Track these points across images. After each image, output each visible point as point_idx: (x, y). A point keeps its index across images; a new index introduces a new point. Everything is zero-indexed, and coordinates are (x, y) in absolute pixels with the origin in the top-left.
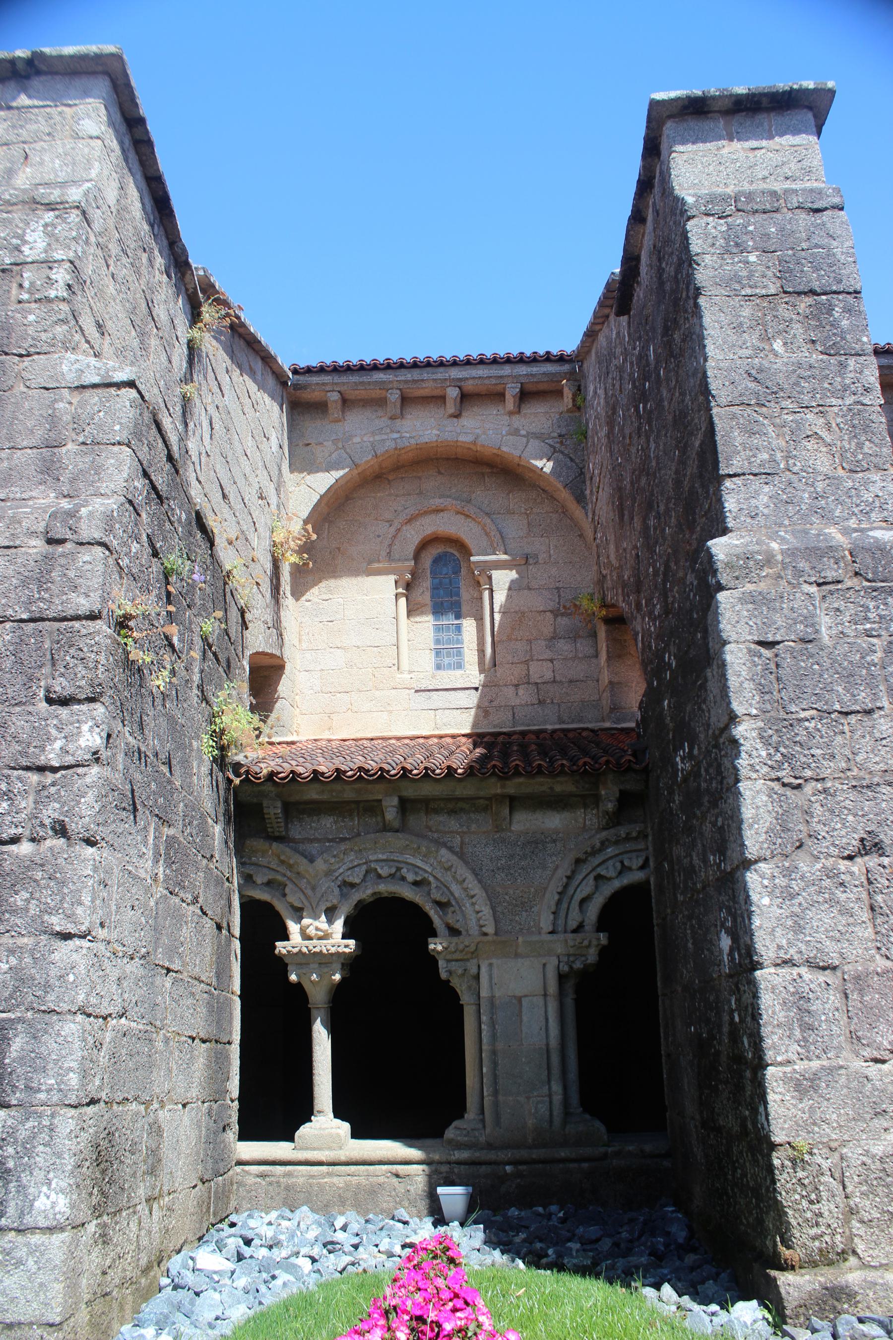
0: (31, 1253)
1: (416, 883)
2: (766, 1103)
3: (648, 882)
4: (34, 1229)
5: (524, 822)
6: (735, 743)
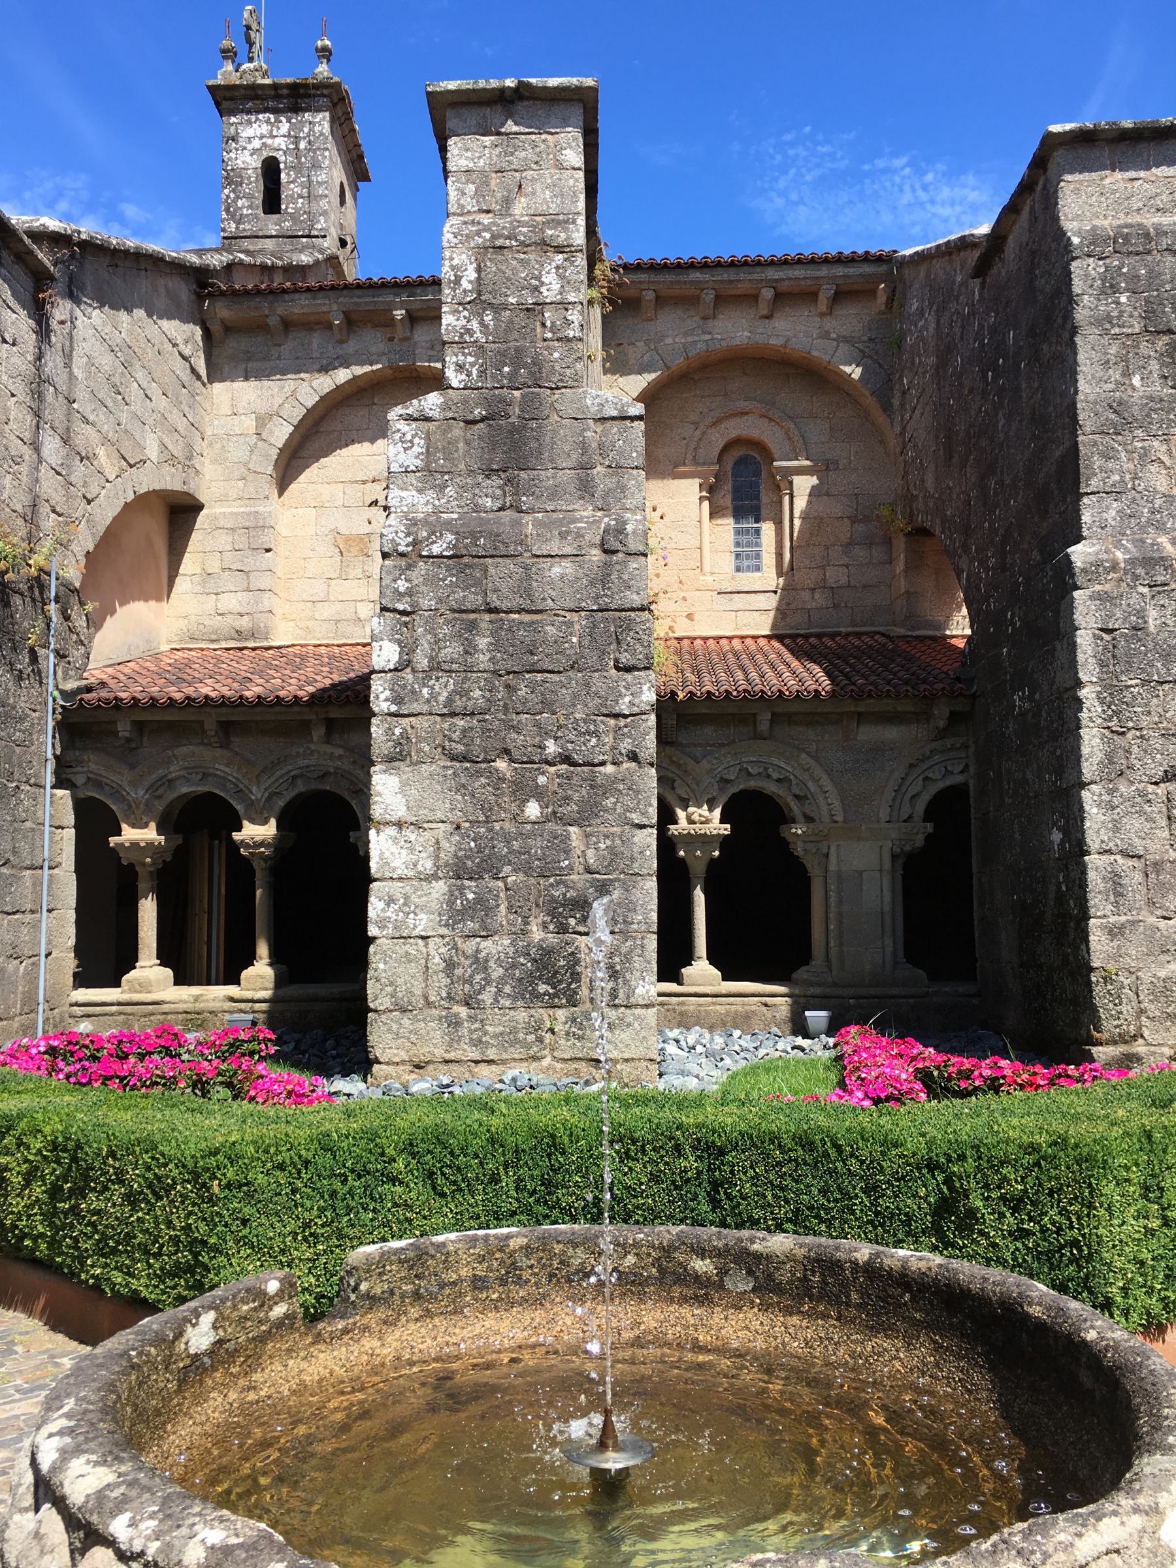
0: (636, 1019)
1: (779, 780)
2: (1087, 942)
3: (966, 784)
4: (636, 1006)
5: (868, 734)
6: (1079, 702)
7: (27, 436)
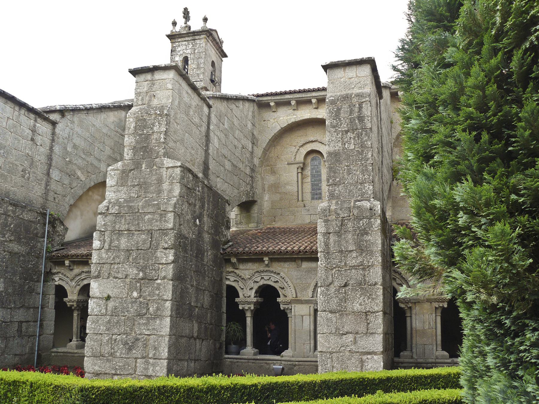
7: (45, 172)
